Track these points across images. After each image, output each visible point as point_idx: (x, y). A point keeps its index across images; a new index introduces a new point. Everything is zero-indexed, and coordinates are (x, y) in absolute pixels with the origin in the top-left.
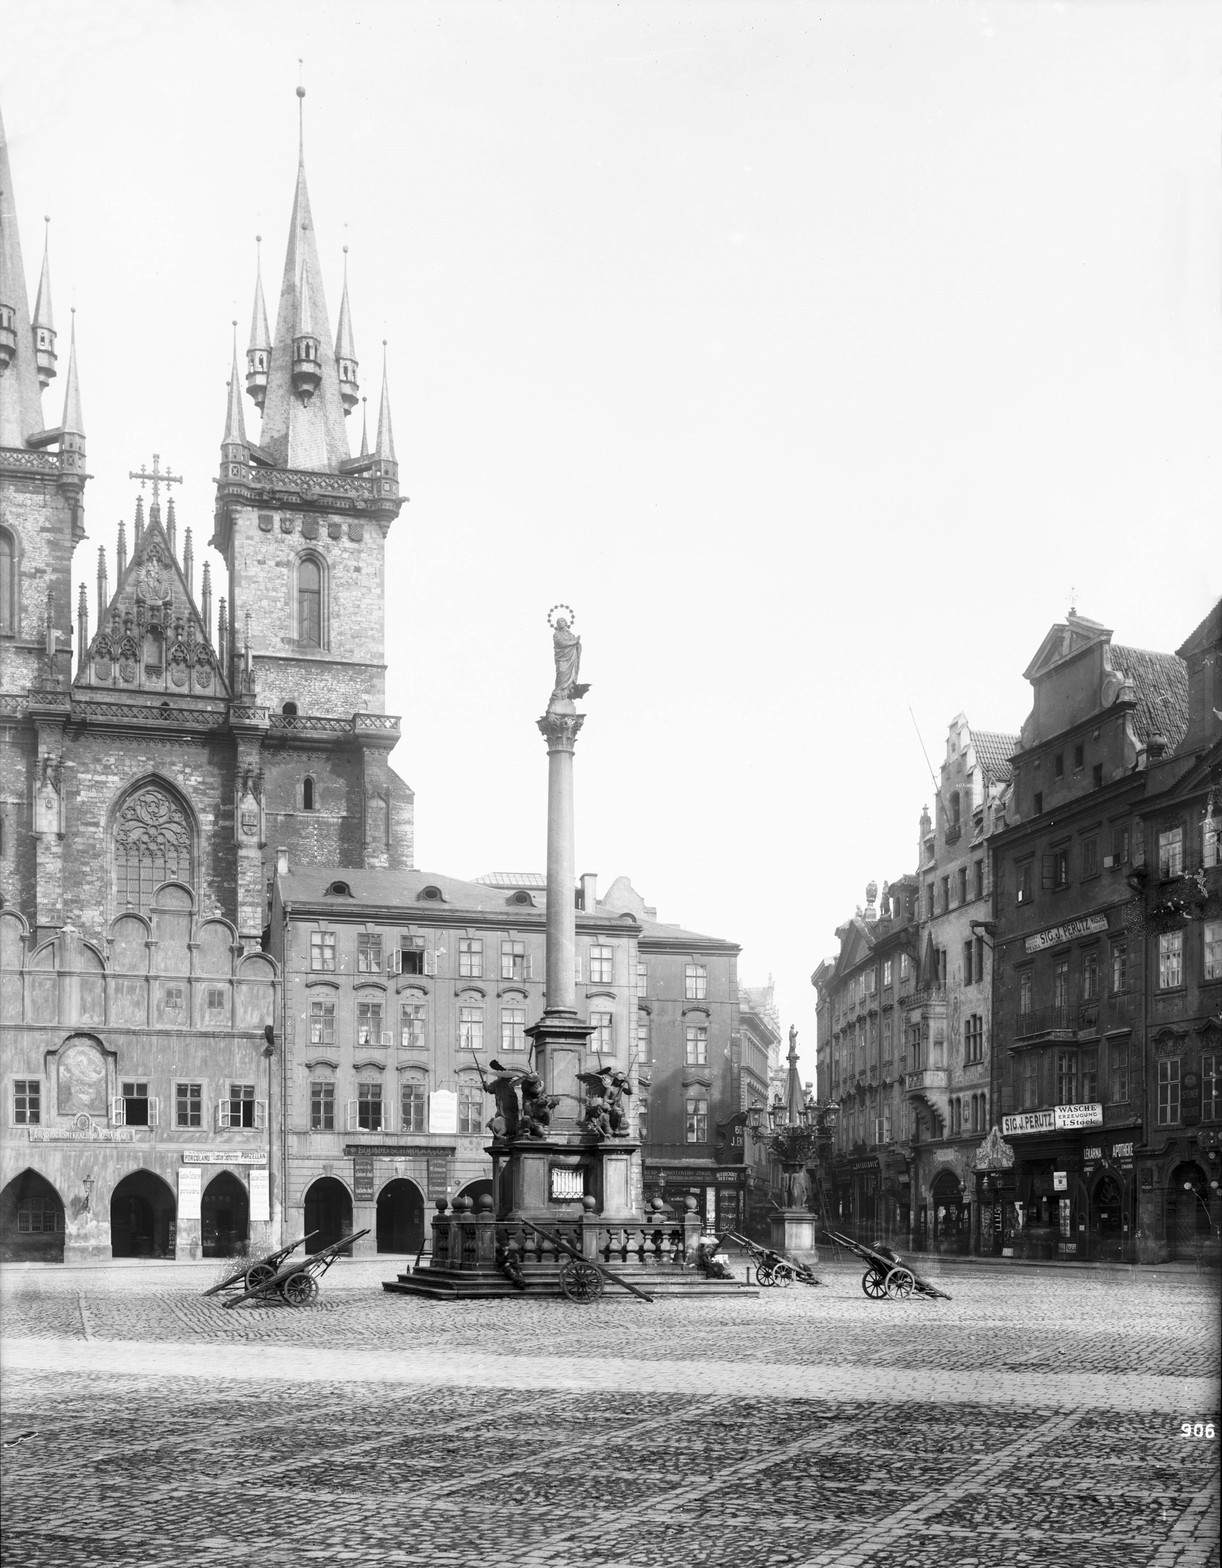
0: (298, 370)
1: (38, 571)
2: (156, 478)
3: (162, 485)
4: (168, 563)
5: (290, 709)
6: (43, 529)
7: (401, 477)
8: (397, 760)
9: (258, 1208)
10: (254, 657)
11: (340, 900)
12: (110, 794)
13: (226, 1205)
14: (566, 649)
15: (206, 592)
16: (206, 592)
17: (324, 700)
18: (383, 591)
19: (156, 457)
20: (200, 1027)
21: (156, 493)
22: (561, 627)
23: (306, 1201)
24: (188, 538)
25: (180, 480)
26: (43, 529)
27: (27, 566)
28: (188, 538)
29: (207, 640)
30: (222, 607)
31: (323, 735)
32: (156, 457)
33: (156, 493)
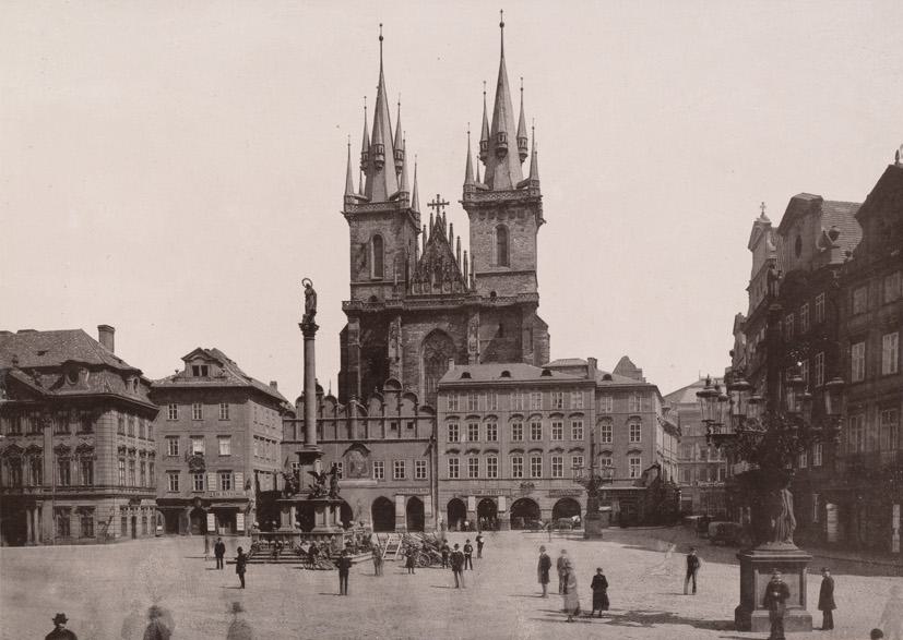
0: (494, 147)
1: (393, 251)
2: (438, 204)
3: (441, 208)
4: (443, 240)
5: (493, 294)
7: (541, 187)
8: (540, 312)
9: (428, 509)
10: (477, 275)
11: (507, 379)
12: (420, 338)
13: (415, 507)
14: (310, 295)
15: (459, 249)
16: (459, 249)
17: (507, 291)
19: (438, 196)
20: (386, 438)
22: (308, 286)
23: (448, 507)
25: (448, 204)
27: (387, 250)
29: (459, 270)
30: (465, 255)
31: (507, 304)
32: (438, 196)
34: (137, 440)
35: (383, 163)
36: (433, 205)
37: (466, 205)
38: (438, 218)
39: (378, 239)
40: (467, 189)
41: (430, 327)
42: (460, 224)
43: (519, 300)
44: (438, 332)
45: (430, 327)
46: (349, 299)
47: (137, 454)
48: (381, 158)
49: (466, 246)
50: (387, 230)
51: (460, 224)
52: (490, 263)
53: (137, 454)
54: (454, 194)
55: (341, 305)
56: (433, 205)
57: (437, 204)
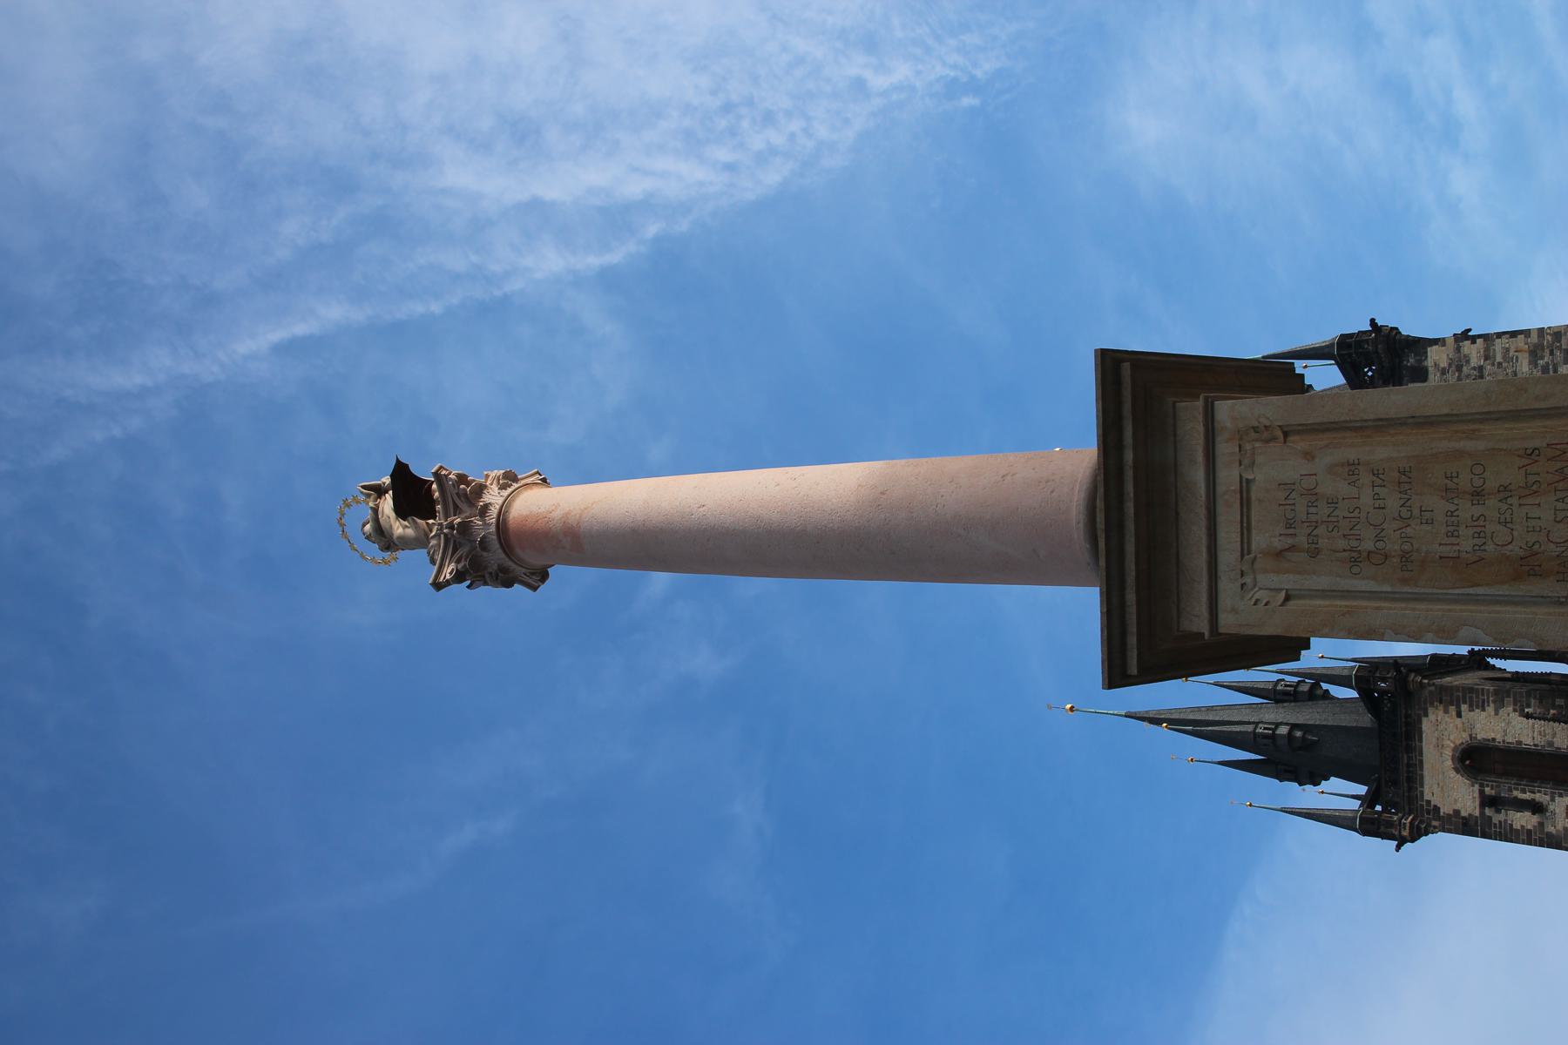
6: (1459, 715)
18: (1480, 336)
26: (1459, 715)
35: (1294, 727)
39: (1476, 759)
48: (1283, 730)
50: (1442, 733)
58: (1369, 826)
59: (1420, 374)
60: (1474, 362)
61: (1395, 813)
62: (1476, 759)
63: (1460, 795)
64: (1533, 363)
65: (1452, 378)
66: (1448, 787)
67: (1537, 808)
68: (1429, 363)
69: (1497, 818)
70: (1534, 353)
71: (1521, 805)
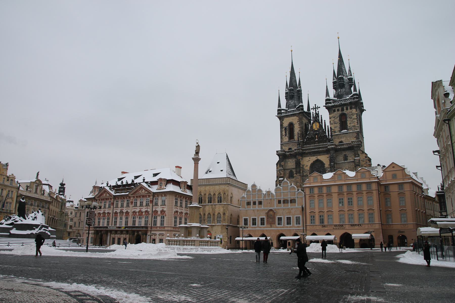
2: (316, 108)
4: (319, 123)
21: (316, 111)
24: (321, 117)
28: (321, 117)
33: (316, 111)
34: (184, 209)
36: (313, 109)
37: (327, 108)
38: (316, 113)
39: (291, 125)
40: (328, 101)
41: (313, 159)
42: (325, 115)
43: (352, 144)
44: (318, 161)
45: (313, 159)
46: (279, 149)
47: (184, 214)
49: (328, 124)
50: (295, 120)
51: (325, 115)
52: (337, 129)
53: (184, 214)
54: (322, 103)
55: (276, 153)
56: (313, 109)
57: (316, 108)
58: (279, 111)
59: (351, 108)
60: (353, 117)
61: (281, 115)
62: (291, 125)
63: (286, 124)
64: (353, 126)
65: (350, 114)
66: (286, 122)
67: (286, 135)
68: (353, 110)
69: (283, 129)
70: (354, 126)
71: (286, 133)
